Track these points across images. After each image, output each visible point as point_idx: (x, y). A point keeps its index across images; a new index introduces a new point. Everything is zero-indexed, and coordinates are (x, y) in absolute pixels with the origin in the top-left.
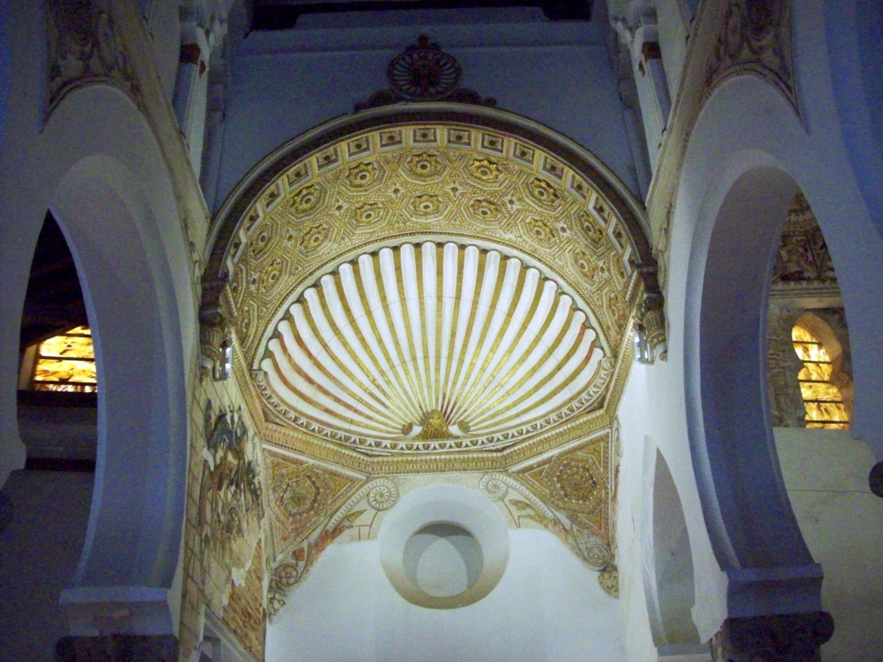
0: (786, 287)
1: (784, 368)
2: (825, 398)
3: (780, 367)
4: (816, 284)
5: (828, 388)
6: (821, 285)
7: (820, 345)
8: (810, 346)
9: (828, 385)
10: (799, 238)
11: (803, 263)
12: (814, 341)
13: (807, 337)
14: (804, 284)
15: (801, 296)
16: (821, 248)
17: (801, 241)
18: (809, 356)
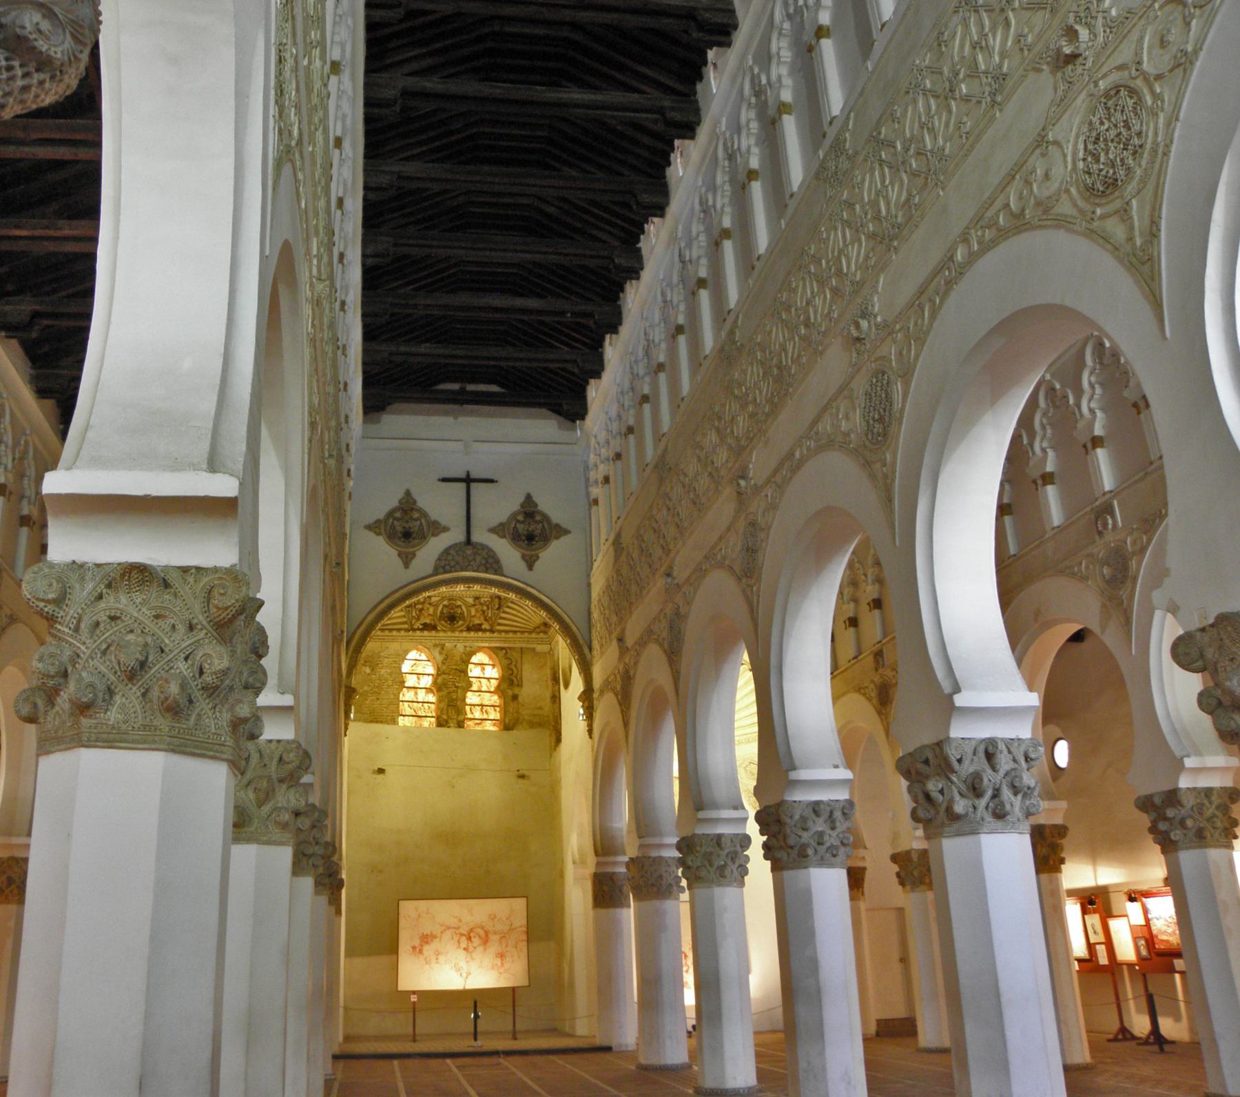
4: (488, 634)
7: (494, 666)
14: (480, 634)
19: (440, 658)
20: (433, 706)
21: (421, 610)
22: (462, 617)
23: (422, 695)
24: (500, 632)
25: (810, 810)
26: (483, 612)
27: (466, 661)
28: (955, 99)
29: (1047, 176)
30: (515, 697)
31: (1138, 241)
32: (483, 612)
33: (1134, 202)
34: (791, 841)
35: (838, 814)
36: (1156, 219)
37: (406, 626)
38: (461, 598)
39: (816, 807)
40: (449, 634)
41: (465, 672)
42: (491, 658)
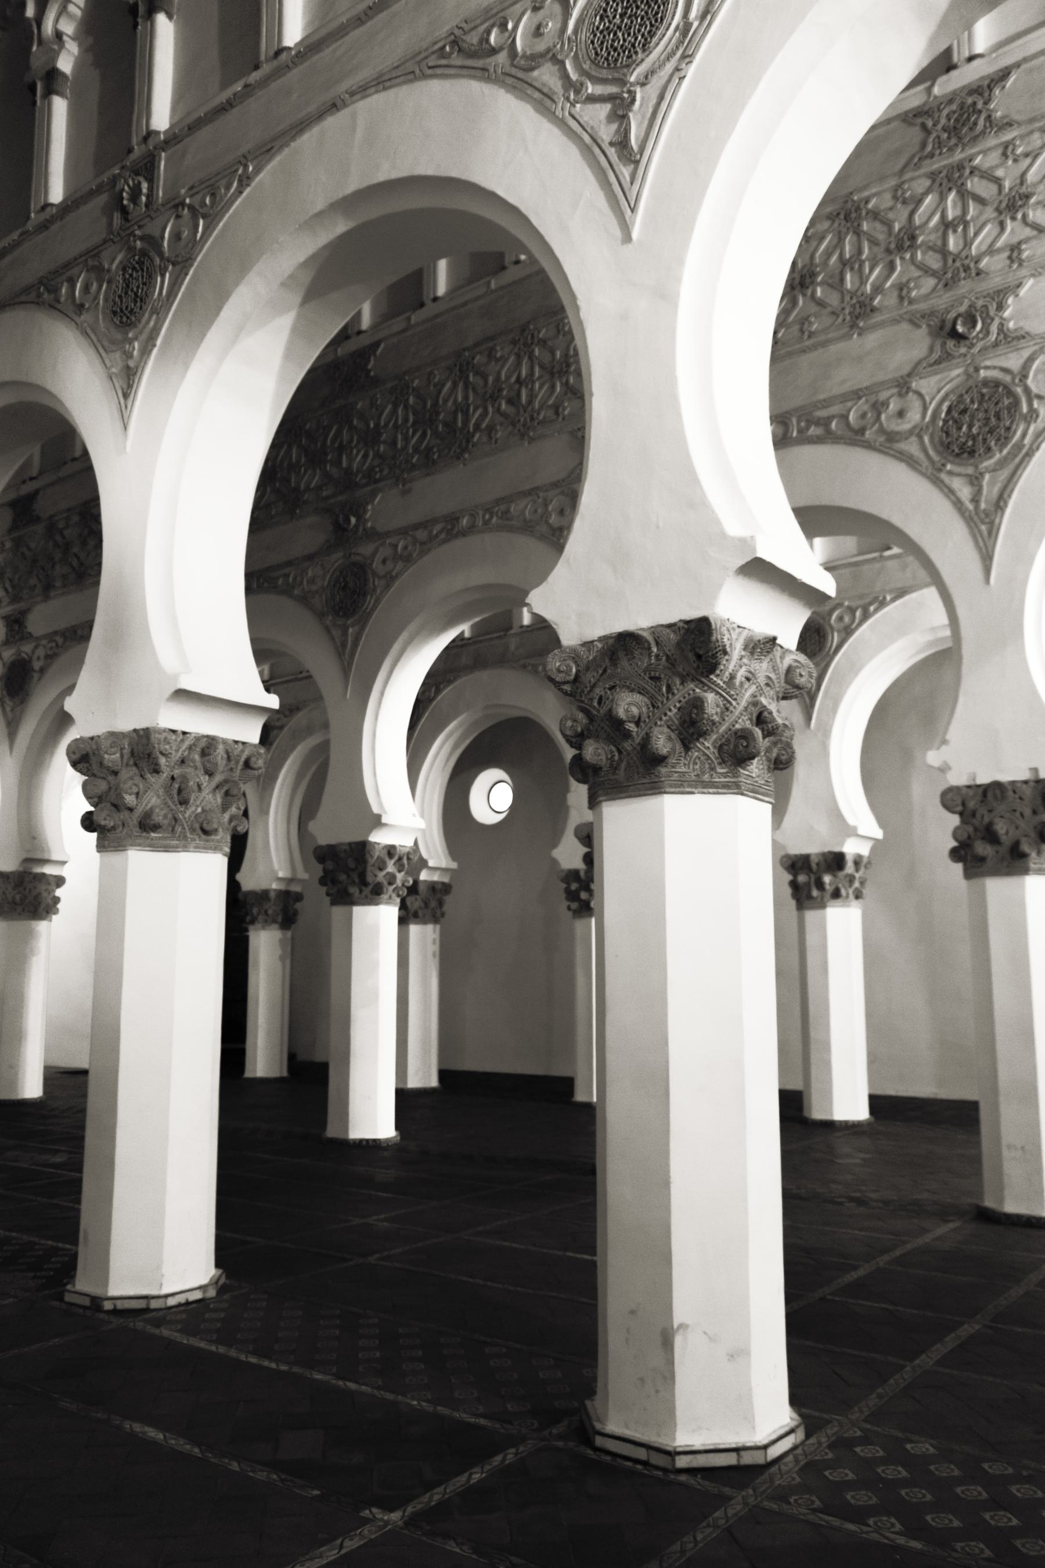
25: (385, 852)
28: (804, 295)
29: (901, 414)
31: (983, 506)
33: (987, 477)
34: (370, 878)
35: (405, 861)
36: (1005, 496)
39: (391, 850)
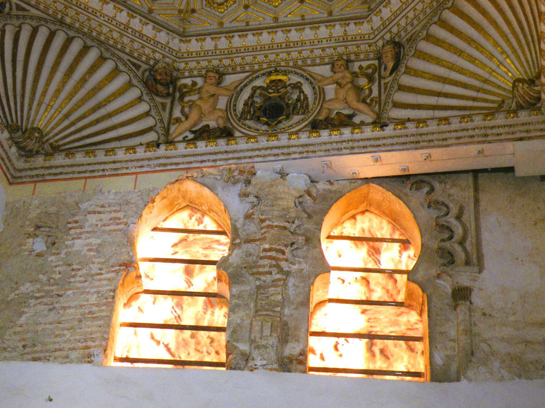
0: (313, 140)
1: (288, 274)
2: (387, 331)
3: (281, 270)
4: (368, 132)
5: (400, 315)
6: (378, 133)
7: (405, 244)
8: (385, 245)
9: (403, 309)
10: (365, 64)
11: (352, 97)
12: (397, 236)
13: (384, 229)
14: (347, 132)
15: (339, 152)
16: (391, 74)
17: (369, 67)
18: (378, 262)
19: (239, 208)
20: (222, 337)
21: (192, 105)
22: (301, 105)
23: (192, 312)
24: (402, 122)
26: (359, 89)
27: (317, 217)
30: (461, 294)
32: (359, 89)
37: (151, 137)
38: (298, 68)
40: (263, 142)
41: (312, 241)
42: (395, 220)
